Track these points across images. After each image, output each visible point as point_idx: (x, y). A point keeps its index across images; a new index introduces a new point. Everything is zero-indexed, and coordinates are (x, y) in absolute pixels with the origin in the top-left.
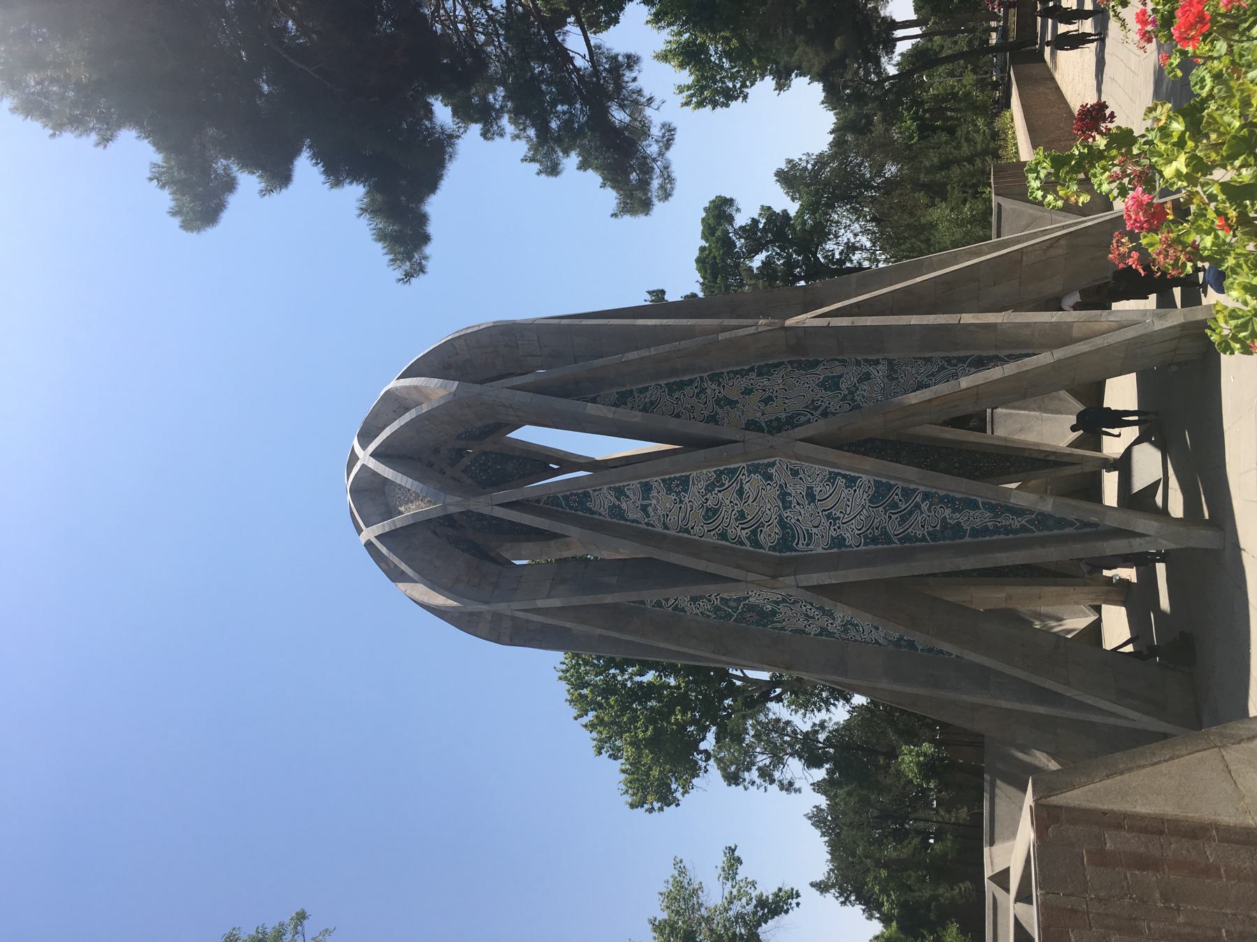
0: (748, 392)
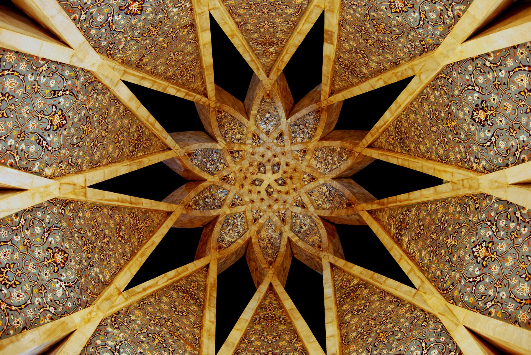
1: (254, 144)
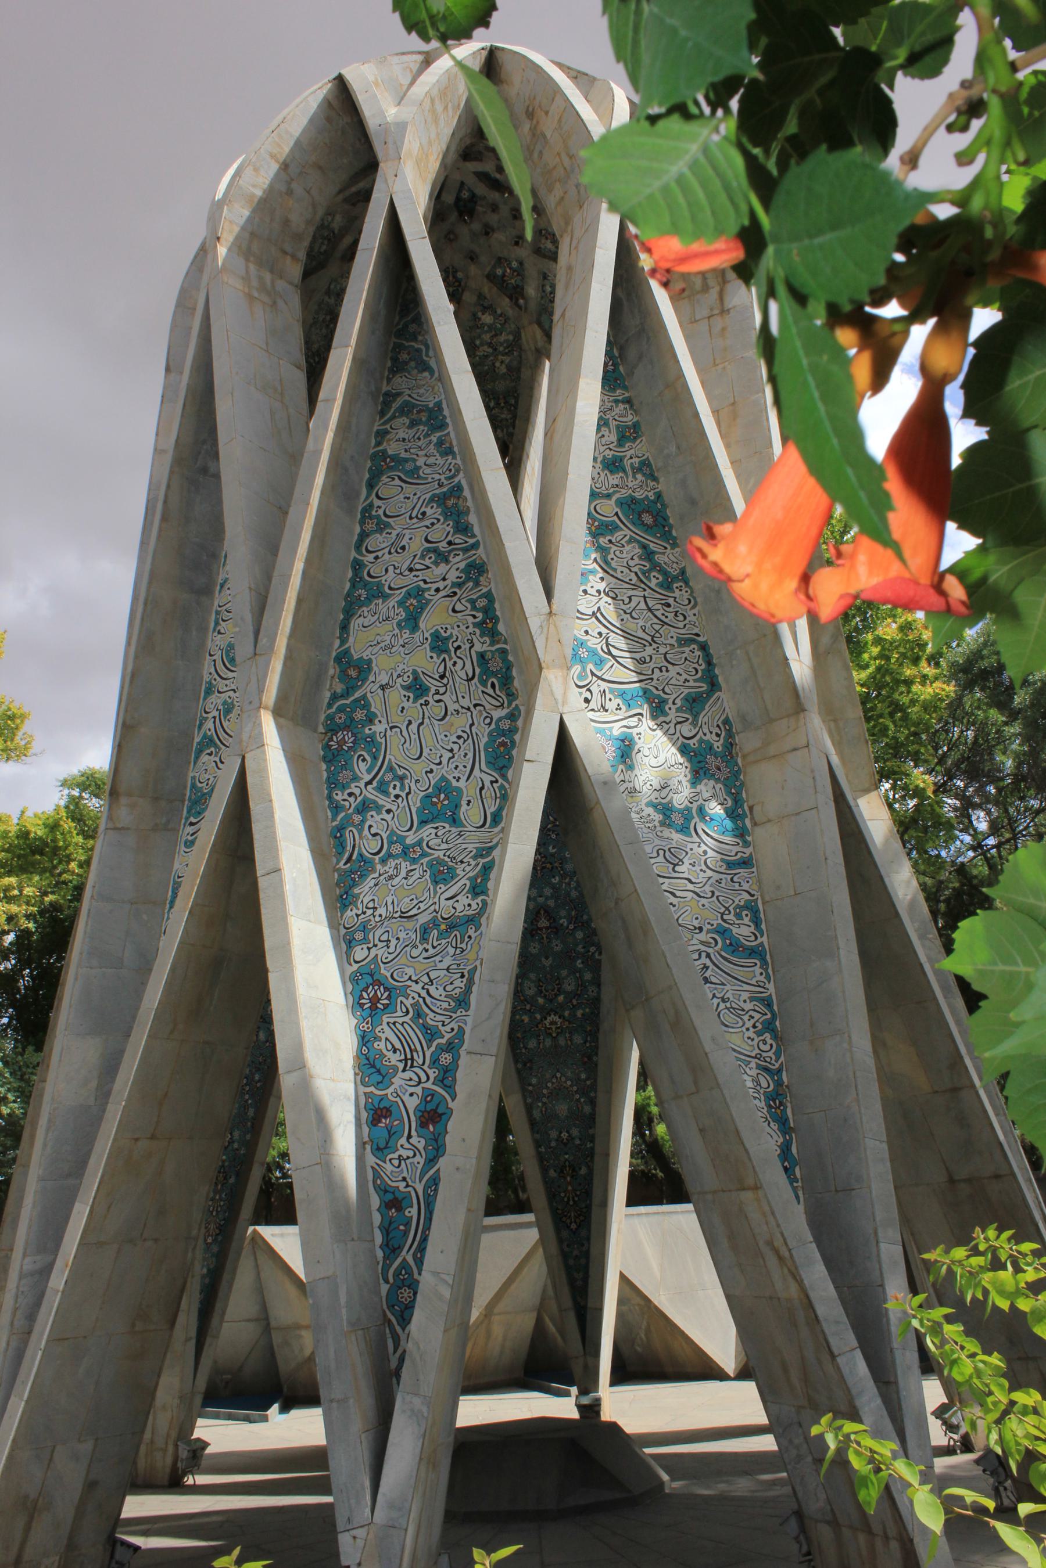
0: (439, 644)
1: (460, 275)
